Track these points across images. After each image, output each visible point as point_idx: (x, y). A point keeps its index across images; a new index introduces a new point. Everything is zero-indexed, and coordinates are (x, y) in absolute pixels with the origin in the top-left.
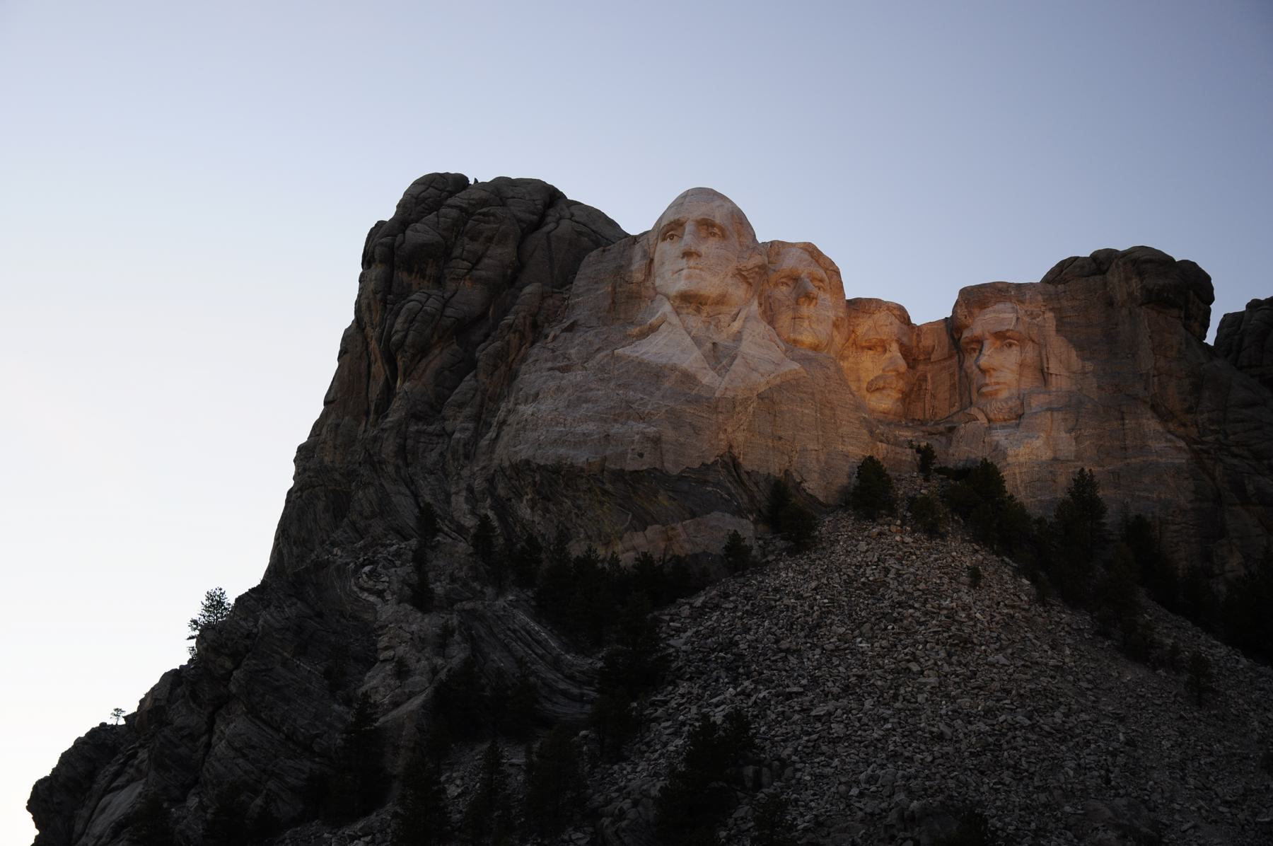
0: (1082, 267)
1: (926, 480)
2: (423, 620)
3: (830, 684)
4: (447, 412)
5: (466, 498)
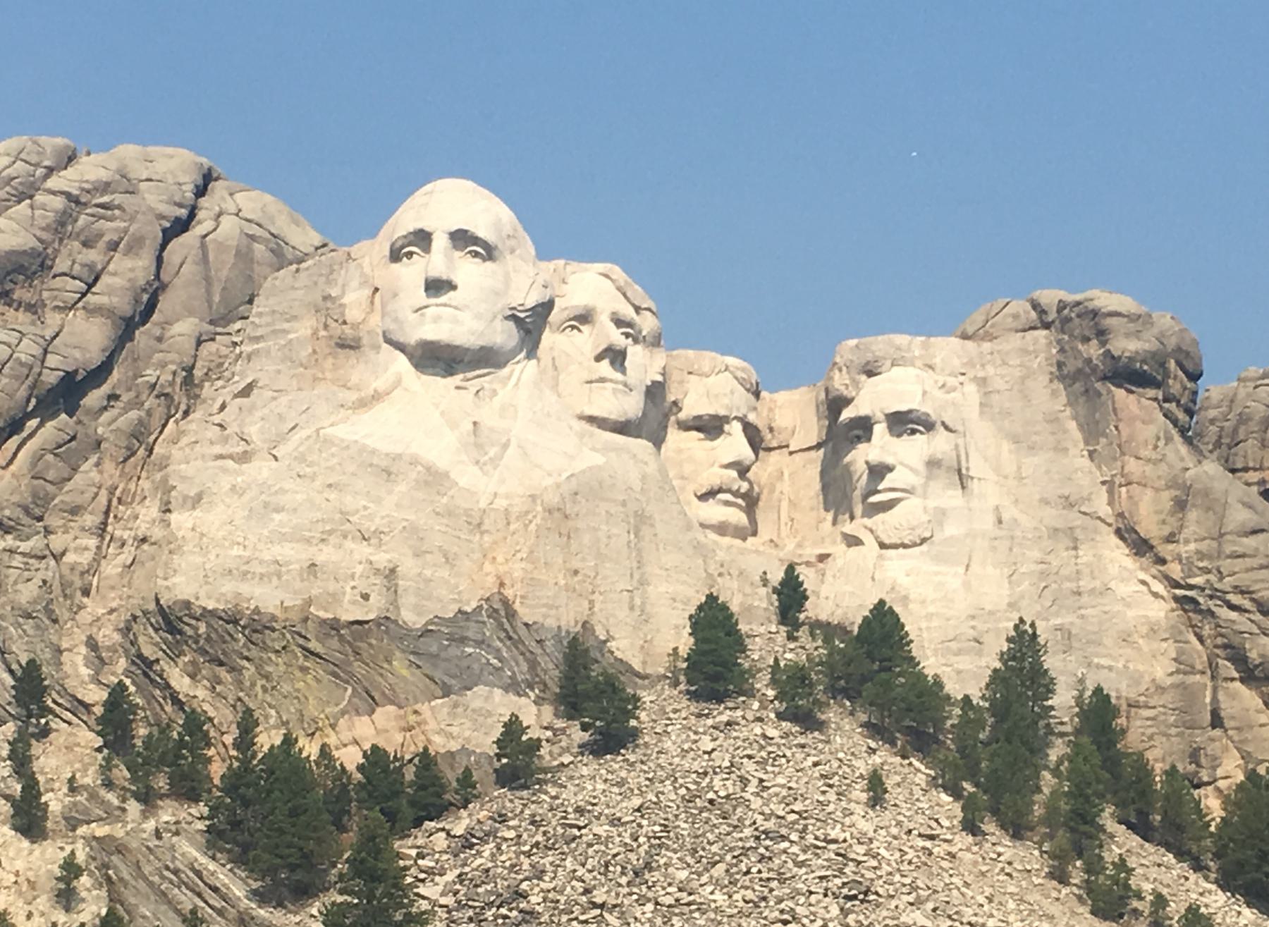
0: (1016, 317)
1: (791, 637)
2: (30, 853)
5: (85, 658)
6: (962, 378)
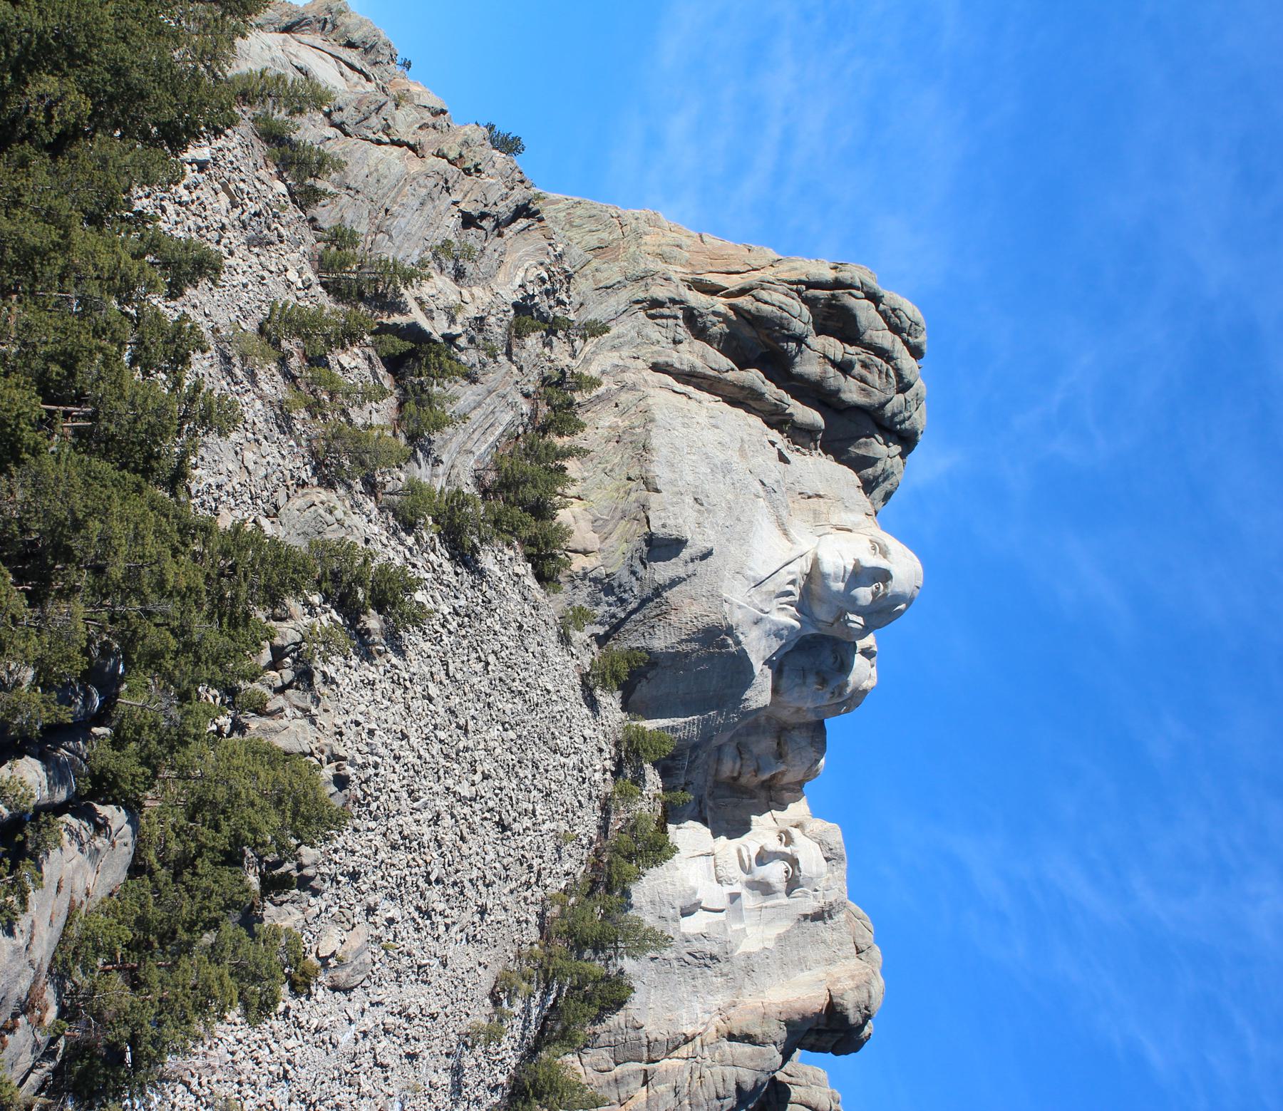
0: (863, 937)
3: (458, 700)
4: (699, 345)
6: (822, 901)
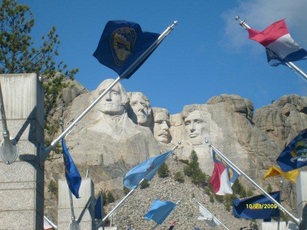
0: (218, 99)
